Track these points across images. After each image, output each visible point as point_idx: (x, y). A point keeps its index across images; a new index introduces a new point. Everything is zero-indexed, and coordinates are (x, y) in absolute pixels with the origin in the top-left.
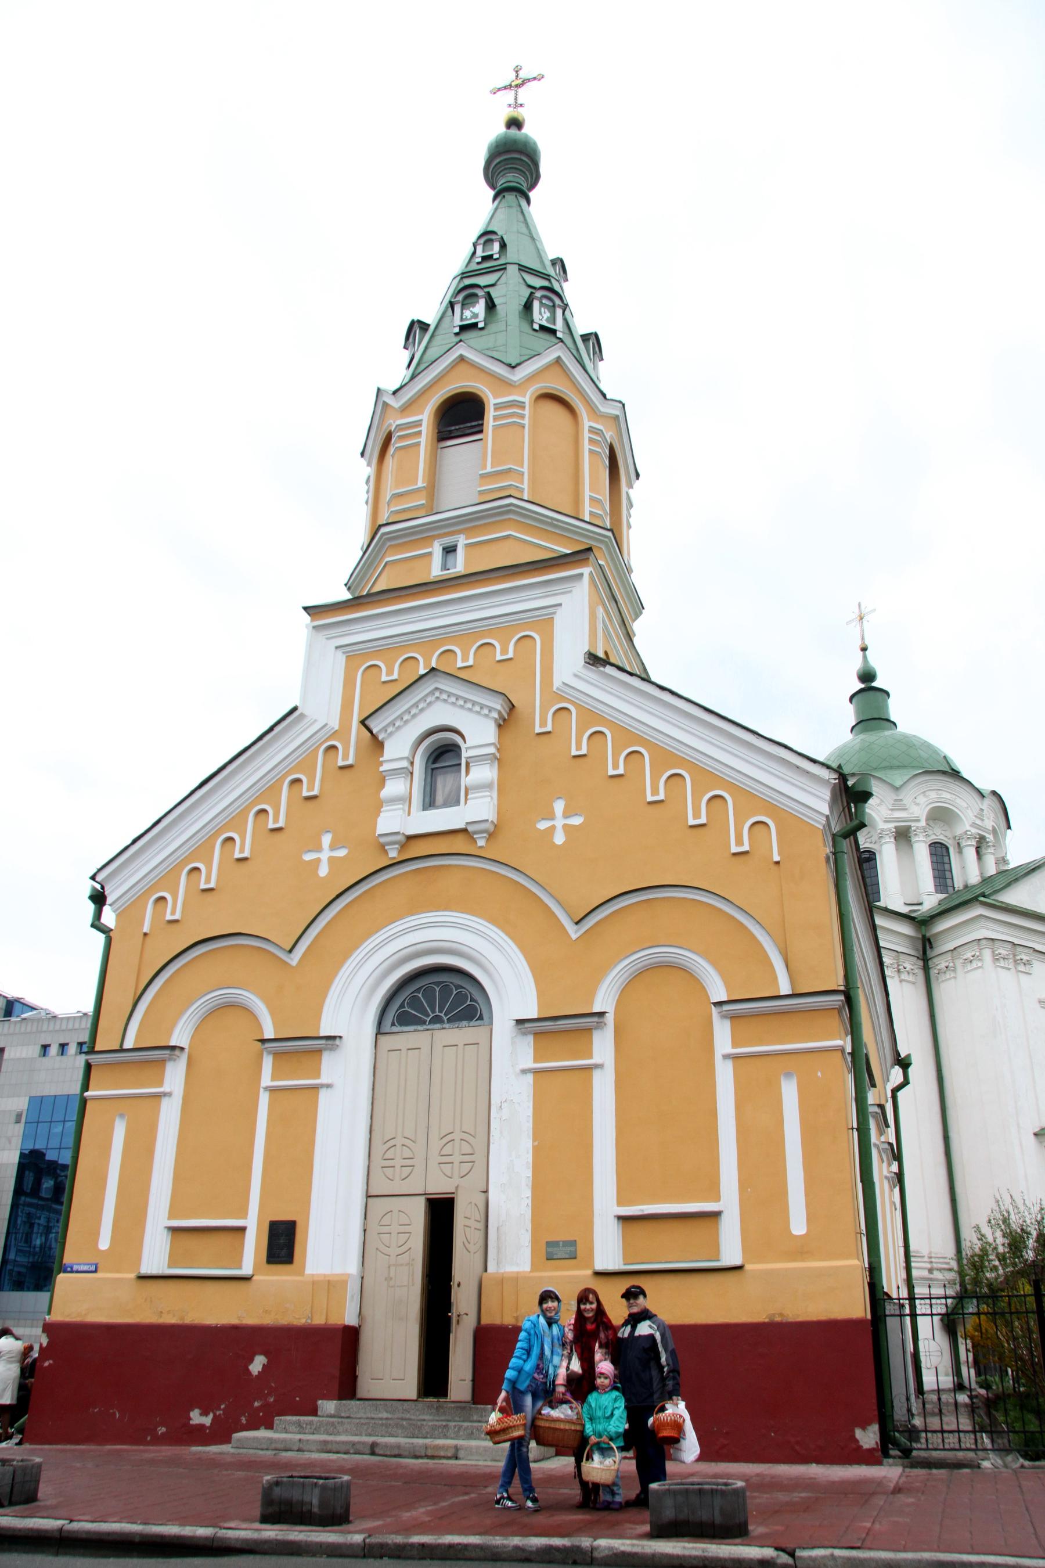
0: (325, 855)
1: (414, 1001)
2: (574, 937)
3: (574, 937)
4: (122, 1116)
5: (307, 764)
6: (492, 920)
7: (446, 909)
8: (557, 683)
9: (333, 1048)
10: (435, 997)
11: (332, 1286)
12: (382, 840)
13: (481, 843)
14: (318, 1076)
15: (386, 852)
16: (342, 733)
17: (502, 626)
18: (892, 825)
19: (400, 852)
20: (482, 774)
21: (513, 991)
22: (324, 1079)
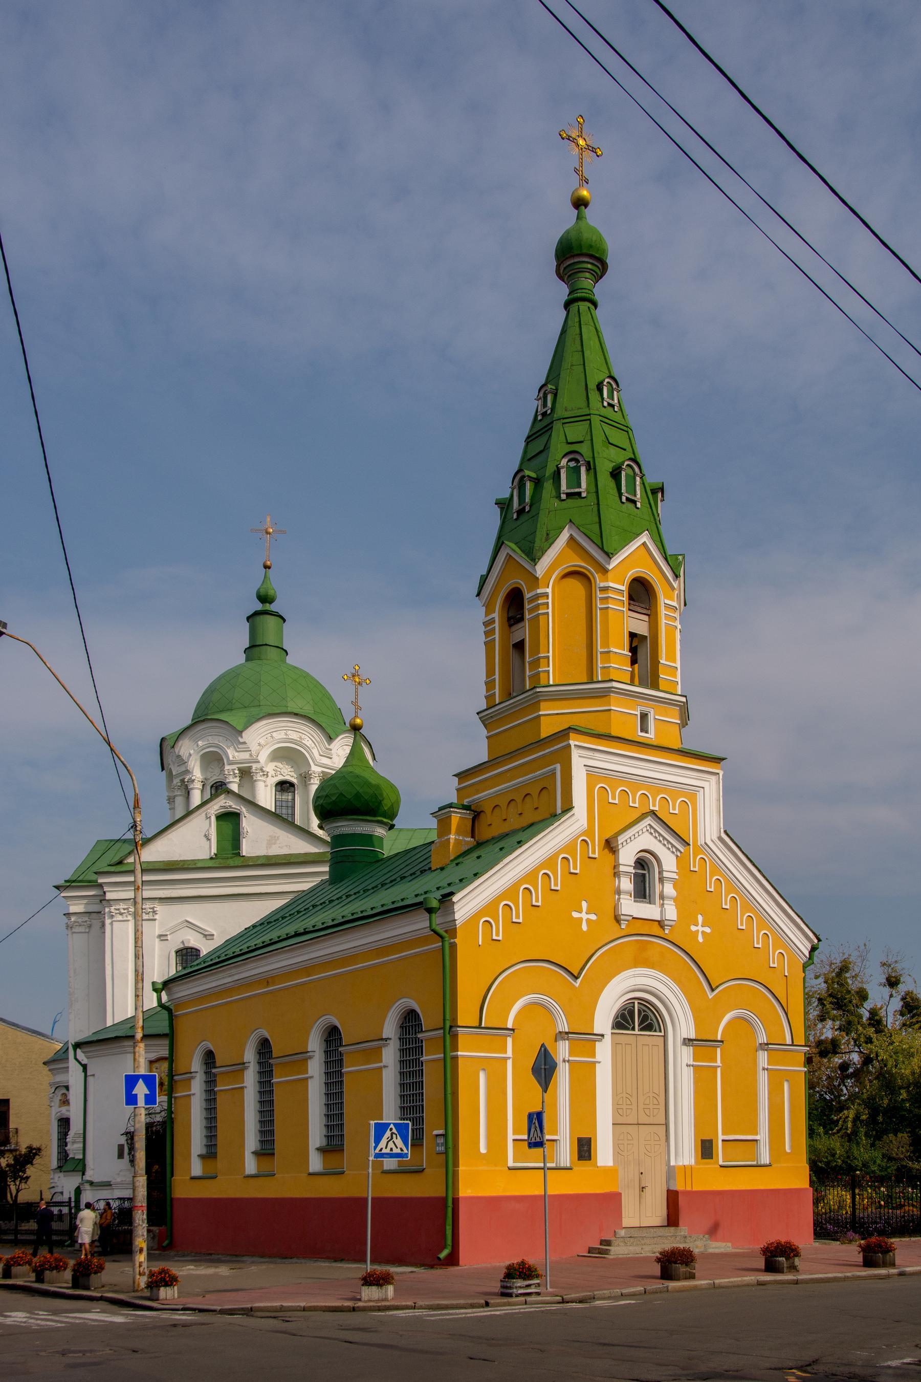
0: (584, 916)
1: (623, 1016)
2: (710, 997)
3: (710, 997)
4: (484, 1069)
5: (570, 847)
6: (674, 980)
7: (653, 968)
8: (701, 841)
9: (600, 1040)
10: (638, 1017)
11: (606, 1170)
12: (622, 917)
13: (667, 932)
14: (594, 1056)
15: (620, 925)
16: (589, 831)
17: (675, 790)
18: (320, 769)
19: (627, 926)
20: (669, 889)
21: (682, 1022)
22: (598, 1058)
